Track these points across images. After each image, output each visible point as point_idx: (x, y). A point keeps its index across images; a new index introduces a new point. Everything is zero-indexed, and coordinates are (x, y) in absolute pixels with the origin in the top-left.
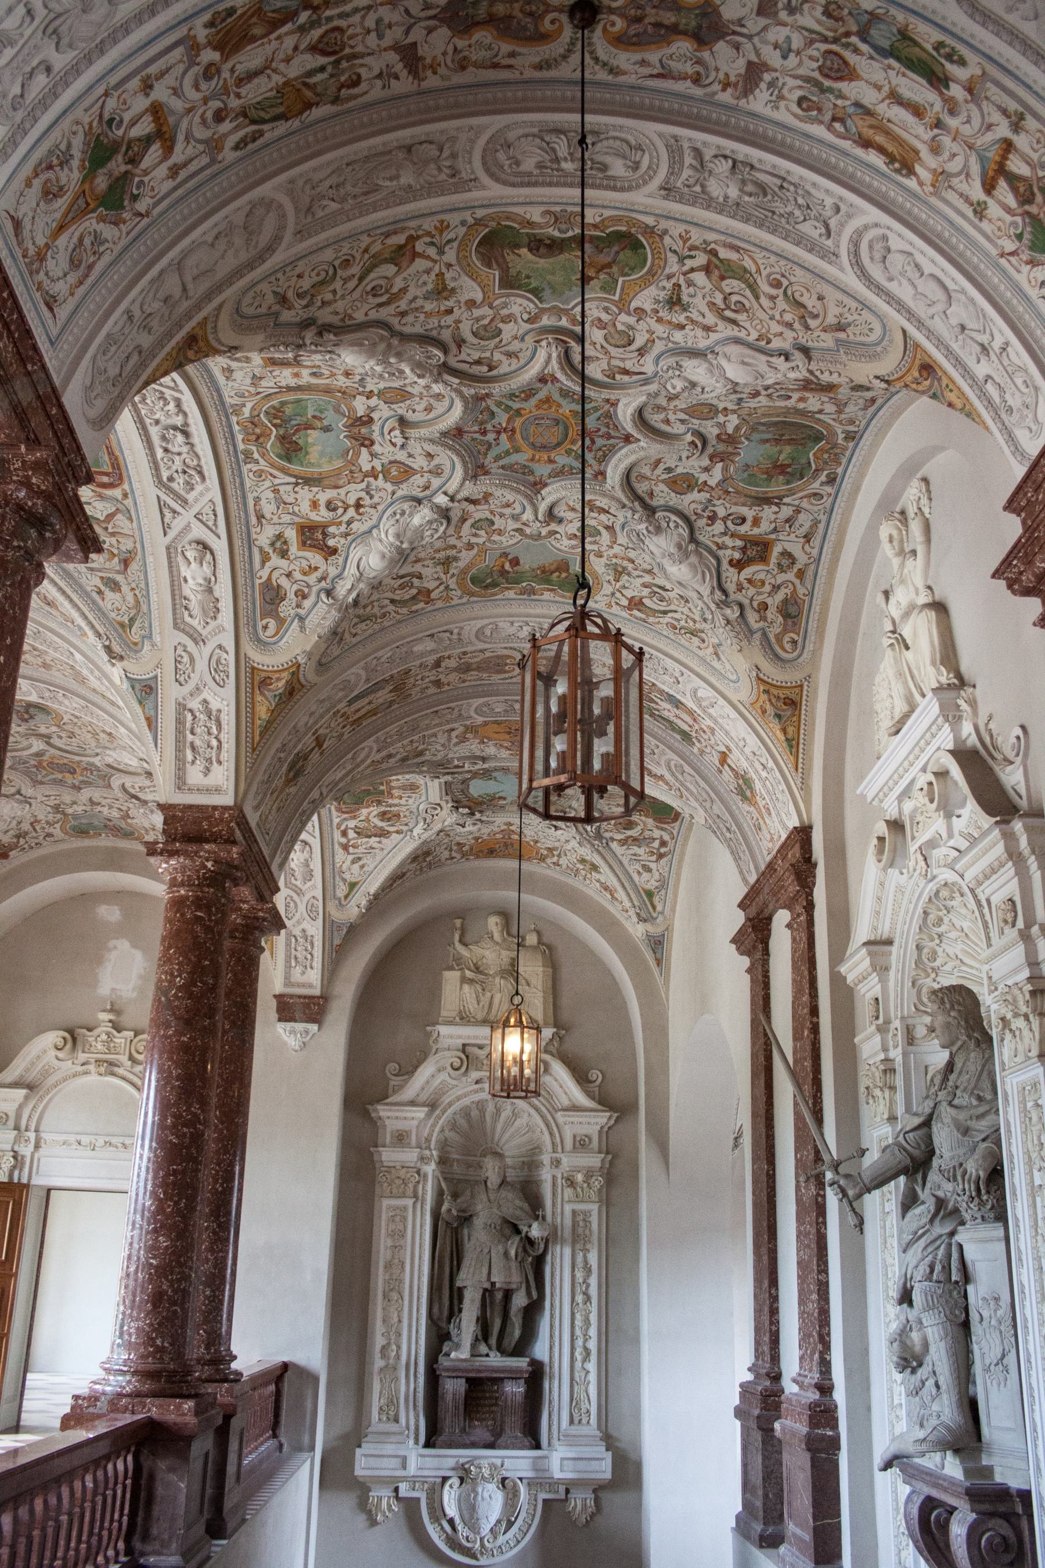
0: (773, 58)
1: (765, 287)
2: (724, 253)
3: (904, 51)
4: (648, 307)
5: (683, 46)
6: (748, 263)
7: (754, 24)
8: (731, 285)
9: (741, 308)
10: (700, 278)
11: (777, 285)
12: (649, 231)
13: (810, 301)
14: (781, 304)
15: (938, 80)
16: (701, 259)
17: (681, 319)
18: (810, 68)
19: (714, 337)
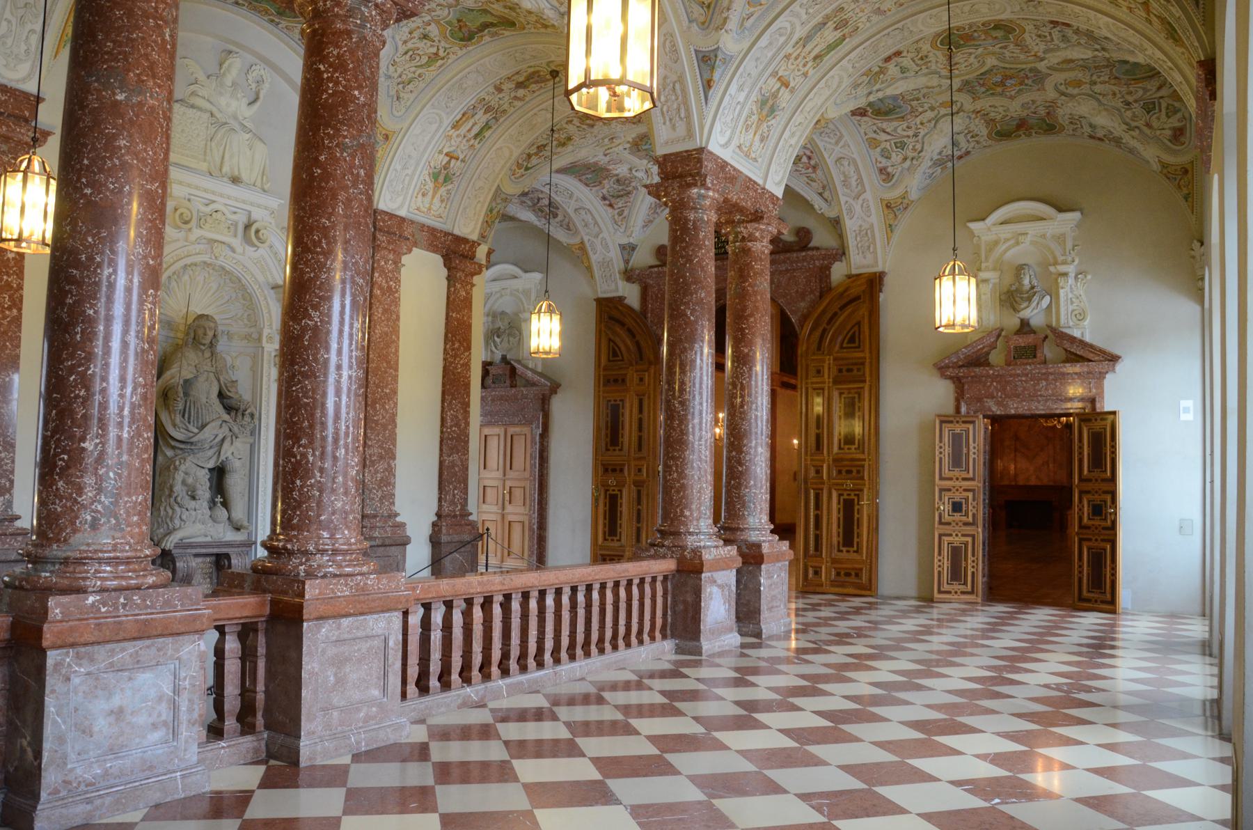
0: (501, 96)
1: (420, 71)
2: (440, 62)
3: (487, 126)
4: (429, 28)
5: (521, 79)
6: (432, 68)
7: (513, 95)
8: (425, 59)
9: (412, 58)
10: (434, 50)
11: (420, 76)
12: (465, 46)
13: (410, 87)
14: (411, 75)
15: (476, 136)
16: (441, 53)
17: (416, 34)
18: (492, 103)
19: (400, 43)
